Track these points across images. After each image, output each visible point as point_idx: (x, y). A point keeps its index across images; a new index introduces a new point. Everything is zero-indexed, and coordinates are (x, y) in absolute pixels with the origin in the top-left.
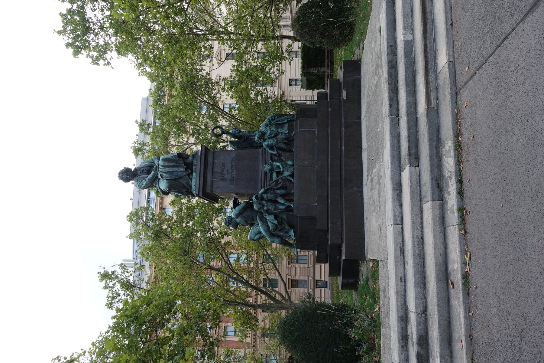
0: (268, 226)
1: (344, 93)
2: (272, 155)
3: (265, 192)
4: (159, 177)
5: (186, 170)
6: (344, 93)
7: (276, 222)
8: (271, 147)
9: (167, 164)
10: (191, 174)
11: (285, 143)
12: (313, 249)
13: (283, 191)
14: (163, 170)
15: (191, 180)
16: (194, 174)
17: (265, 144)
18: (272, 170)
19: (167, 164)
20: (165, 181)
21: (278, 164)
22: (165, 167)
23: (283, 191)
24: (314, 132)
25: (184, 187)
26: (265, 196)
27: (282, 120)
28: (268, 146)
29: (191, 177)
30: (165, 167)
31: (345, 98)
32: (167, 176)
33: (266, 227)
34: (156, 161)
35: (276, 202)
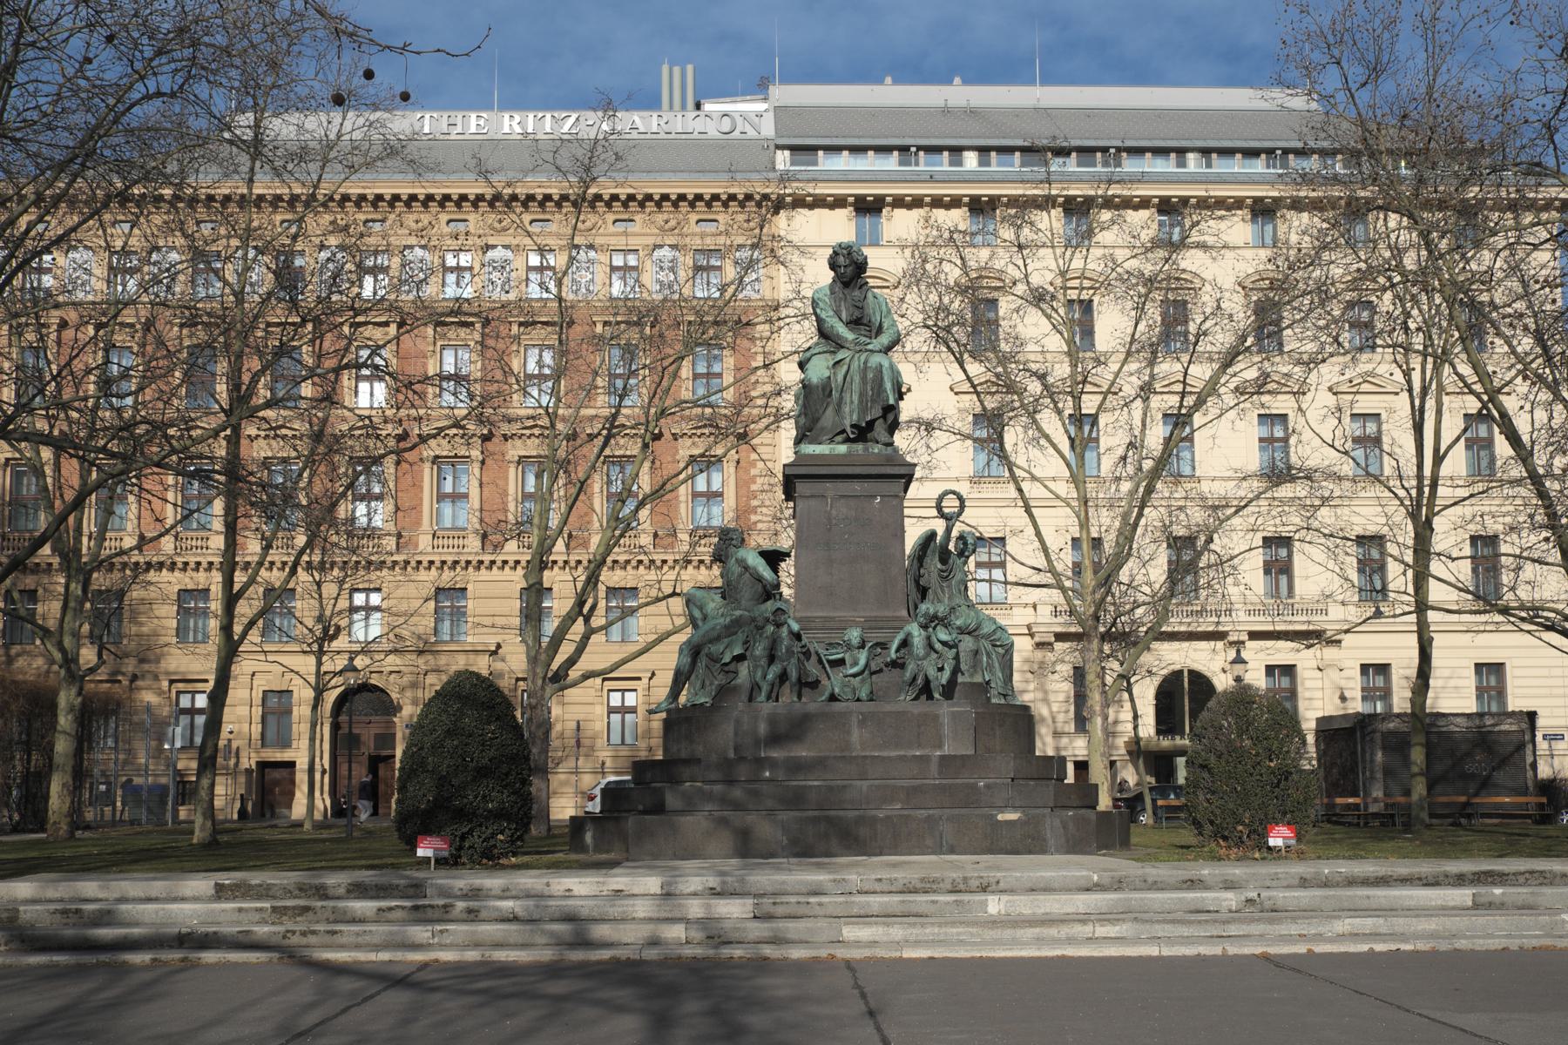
0: (718, 639)
1: (1012, 816)
2: (884, 646)
3: (791, 632)
4: (839, 356)
5: (853, 426)
6: (1012, 816)
7: (727, 659)
8: (905, 643)
9: (870, 375)
10: (848, 440)
11: (914, 679)
12: (666, 750)
13: (794, 675)
14: (855, 365)
15: (831, 441)
16: (843, 449)
17: (914, 629)
18: (849, 647)
19: (870, 375)
20: (827, 374)
21: (862, 662)
22: (865, 369)
23: (794, 675)
24: (940, 746)
25: (816, 420)
26: (784, 631)
27: (990, 667)
28: (909, 635)
29: (839, 438)
30: (865, 369)
31: (1000, 817)
32: (840, 378)
33: (715, 634)
34: (884, 339)
35: (772, 659)
